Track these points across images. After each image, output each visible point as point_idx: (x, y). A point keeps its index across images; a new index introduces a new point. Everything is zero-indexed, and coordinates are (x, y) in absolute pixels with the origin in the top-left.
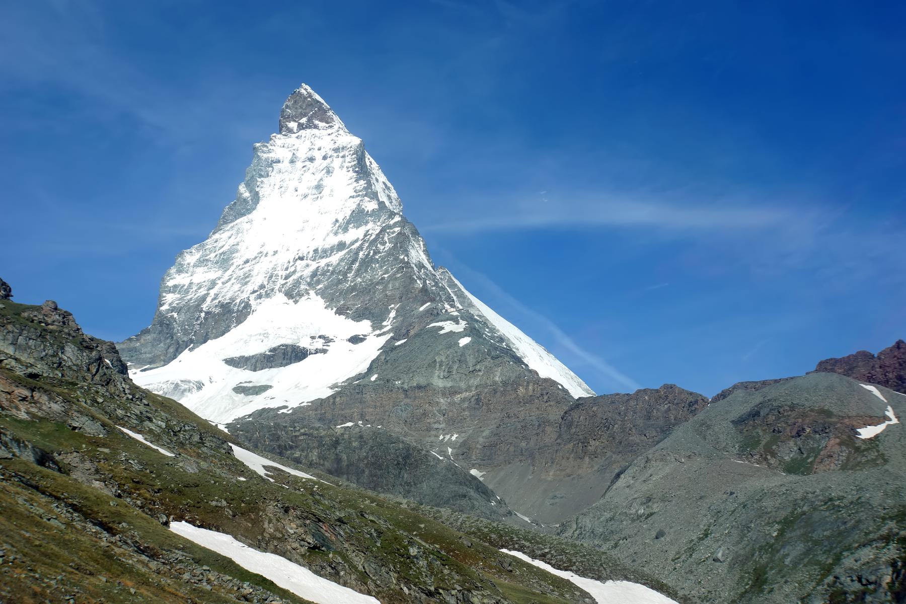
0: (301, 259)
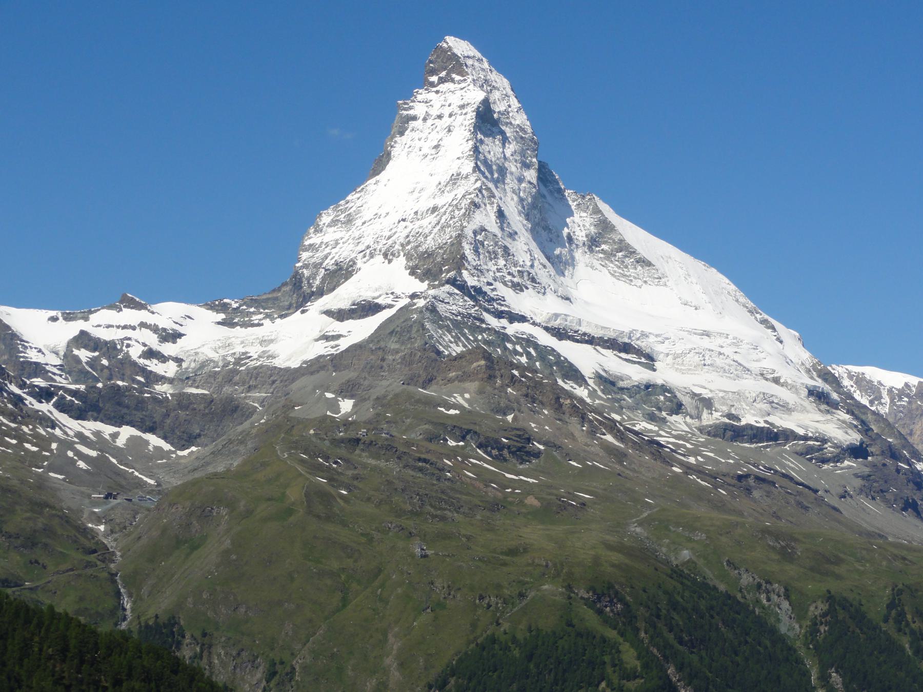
0: (404, 220)
